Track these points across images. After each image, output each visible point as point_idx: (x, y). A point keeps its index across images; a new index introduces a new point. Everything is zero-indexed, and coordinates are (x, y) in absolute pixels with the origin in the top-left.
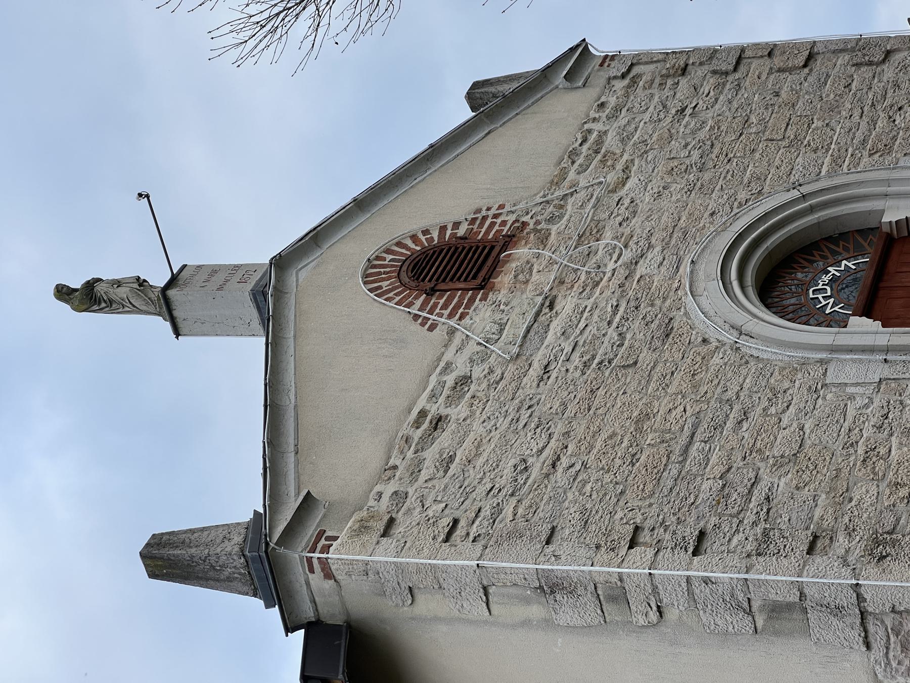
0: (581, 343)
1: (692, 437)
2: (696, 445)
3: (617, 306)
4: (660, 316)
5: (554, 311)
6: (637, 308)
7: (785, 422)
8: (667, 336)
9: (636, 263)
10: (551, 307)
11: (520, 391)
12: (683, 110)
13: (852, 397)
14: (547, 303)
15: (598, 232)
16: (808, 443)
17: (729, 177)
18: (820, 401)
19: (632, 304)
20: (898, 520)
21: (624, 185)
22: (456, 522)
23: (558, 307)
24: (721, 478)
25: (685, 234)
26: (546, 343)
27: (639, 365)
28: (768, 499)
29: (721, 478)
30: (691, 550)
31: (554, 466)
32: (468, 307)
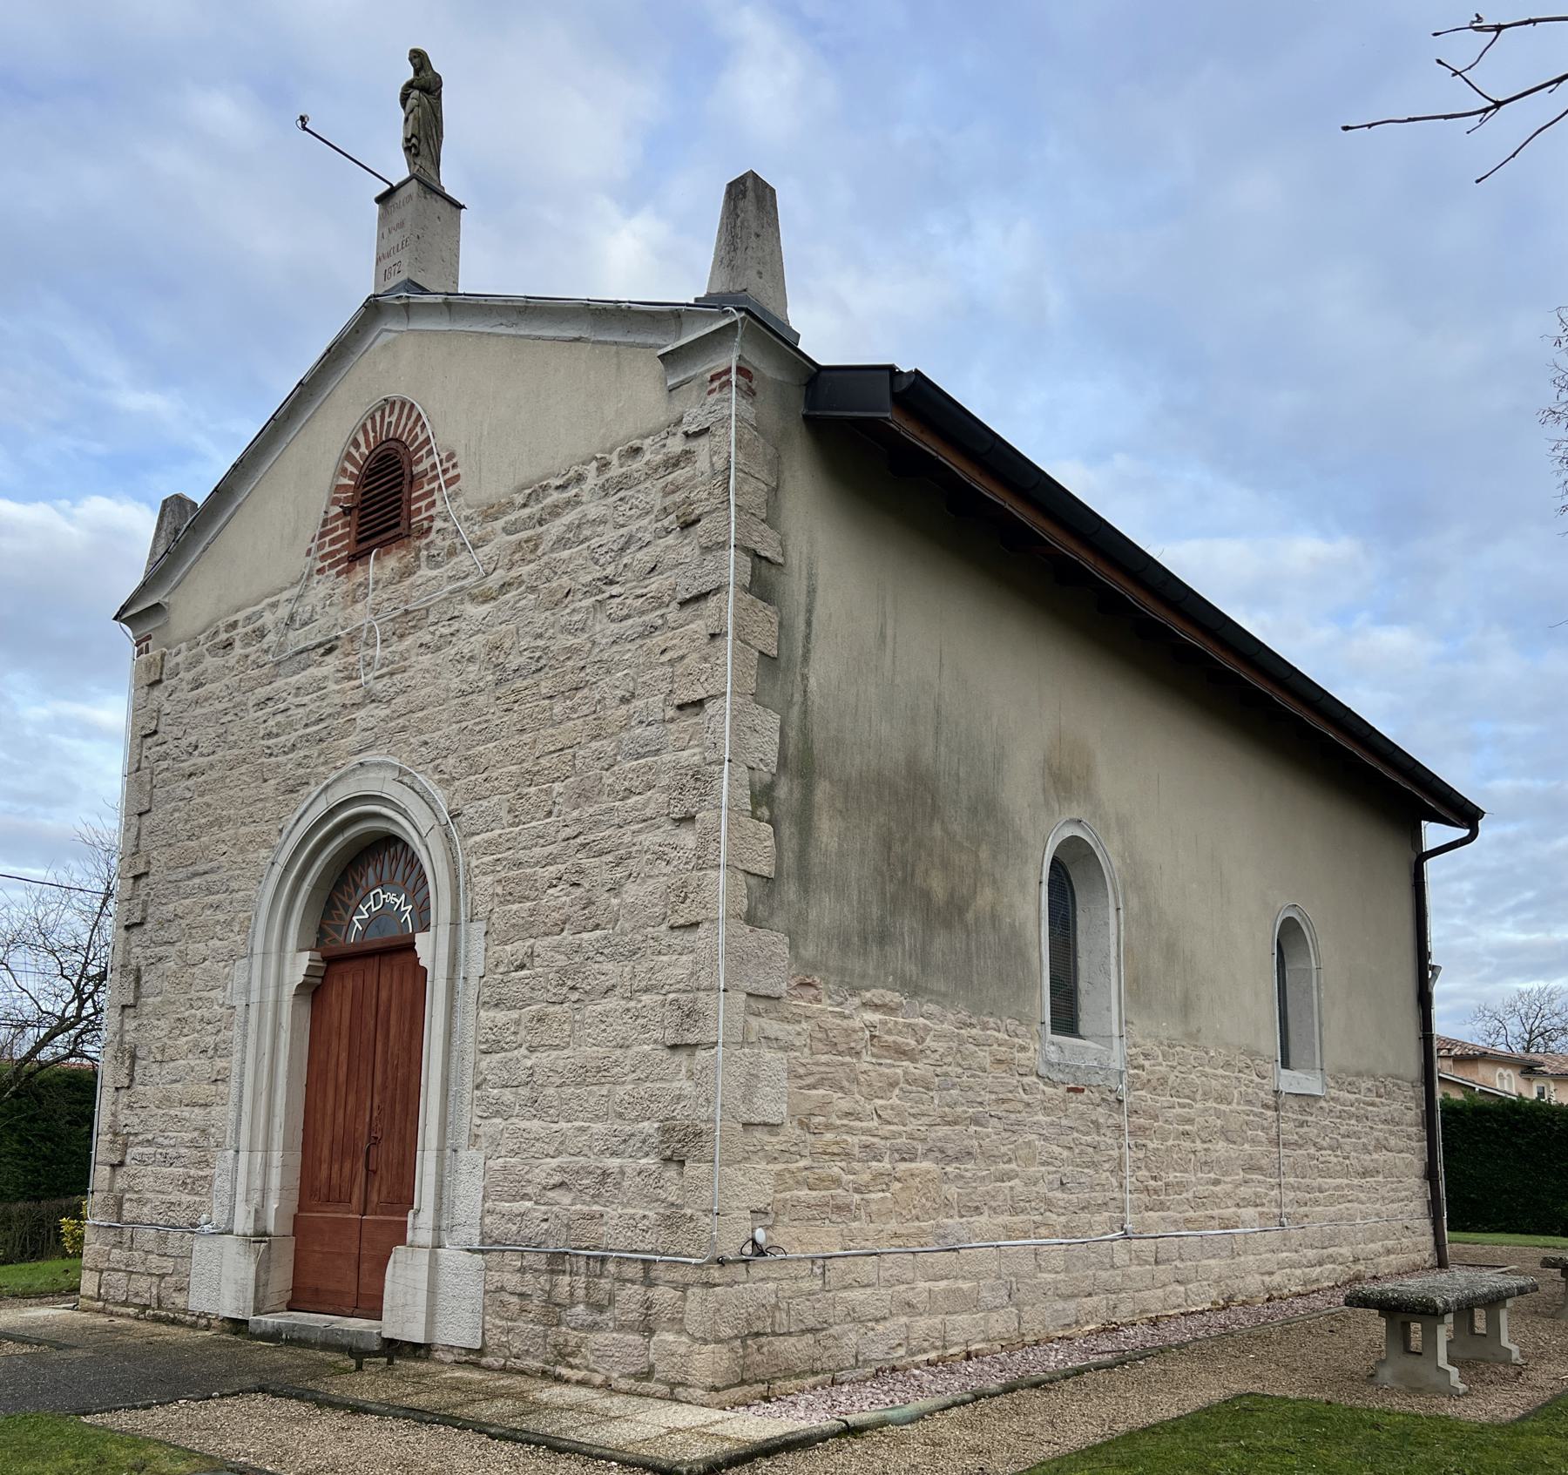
0: (289, 713)
1: (204, 873)
2: (197, 881)
3: (322, 720)
4: (309, 770)
5: (321, 659)
6: (320, 740)
7: (210, 943)
8: (292, 791)
9: (373, 701)
10: (330, 651)
11: (250, 693)
12: (612, 583)
13: (225, 989)
14: (328, 646)
15: (414, 627)
16: (194, 970)
17: (477, 729)
18: (224, 963)
19: (324, 734)
20: (144, 1059)
21: (484, 602)
22: (155, 732)
23: (328, 659)
24: (176, 915)
25: (403, 729)
26: (289, 680)
27: (264, 785)
28: (160, 959)
29: (176, 915)
30: (127, 923)
31: (190, 776)
32: (331, 566)
